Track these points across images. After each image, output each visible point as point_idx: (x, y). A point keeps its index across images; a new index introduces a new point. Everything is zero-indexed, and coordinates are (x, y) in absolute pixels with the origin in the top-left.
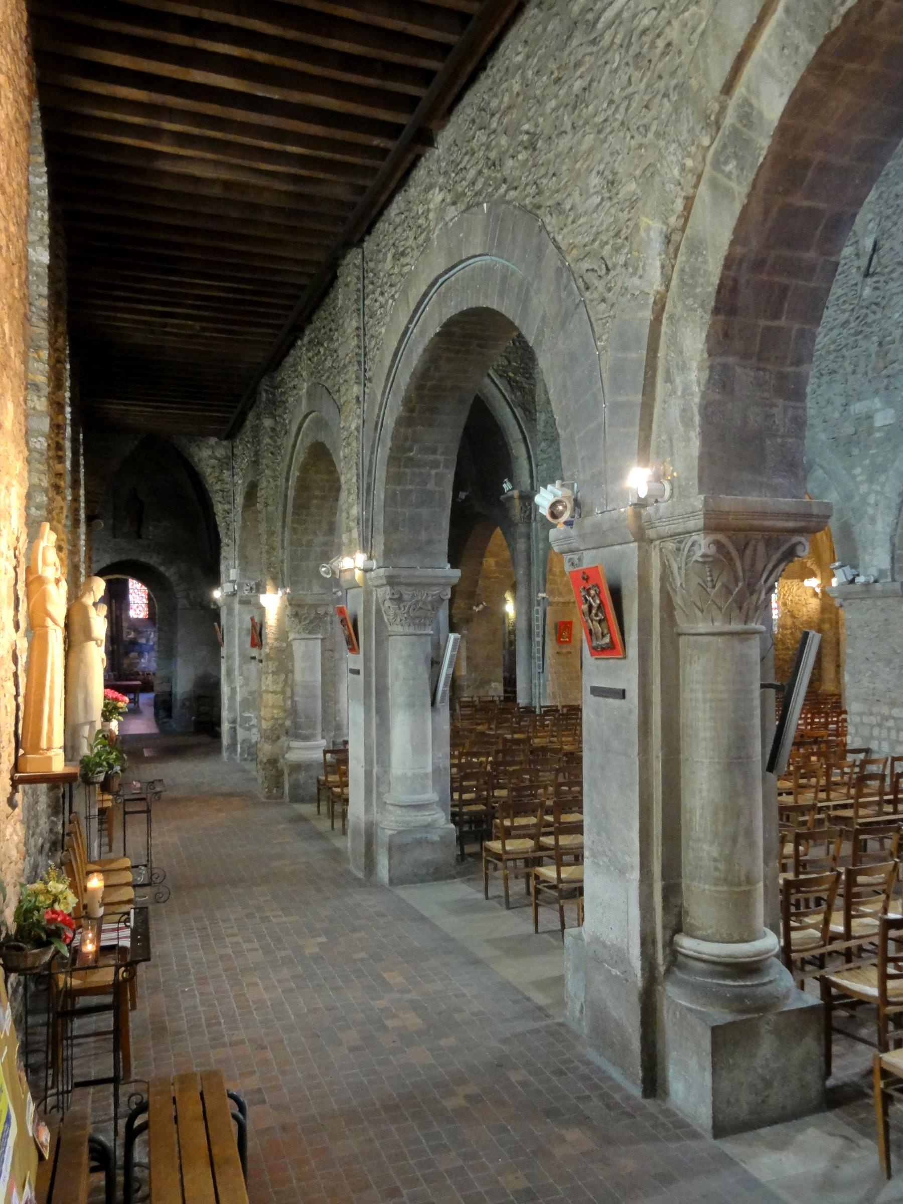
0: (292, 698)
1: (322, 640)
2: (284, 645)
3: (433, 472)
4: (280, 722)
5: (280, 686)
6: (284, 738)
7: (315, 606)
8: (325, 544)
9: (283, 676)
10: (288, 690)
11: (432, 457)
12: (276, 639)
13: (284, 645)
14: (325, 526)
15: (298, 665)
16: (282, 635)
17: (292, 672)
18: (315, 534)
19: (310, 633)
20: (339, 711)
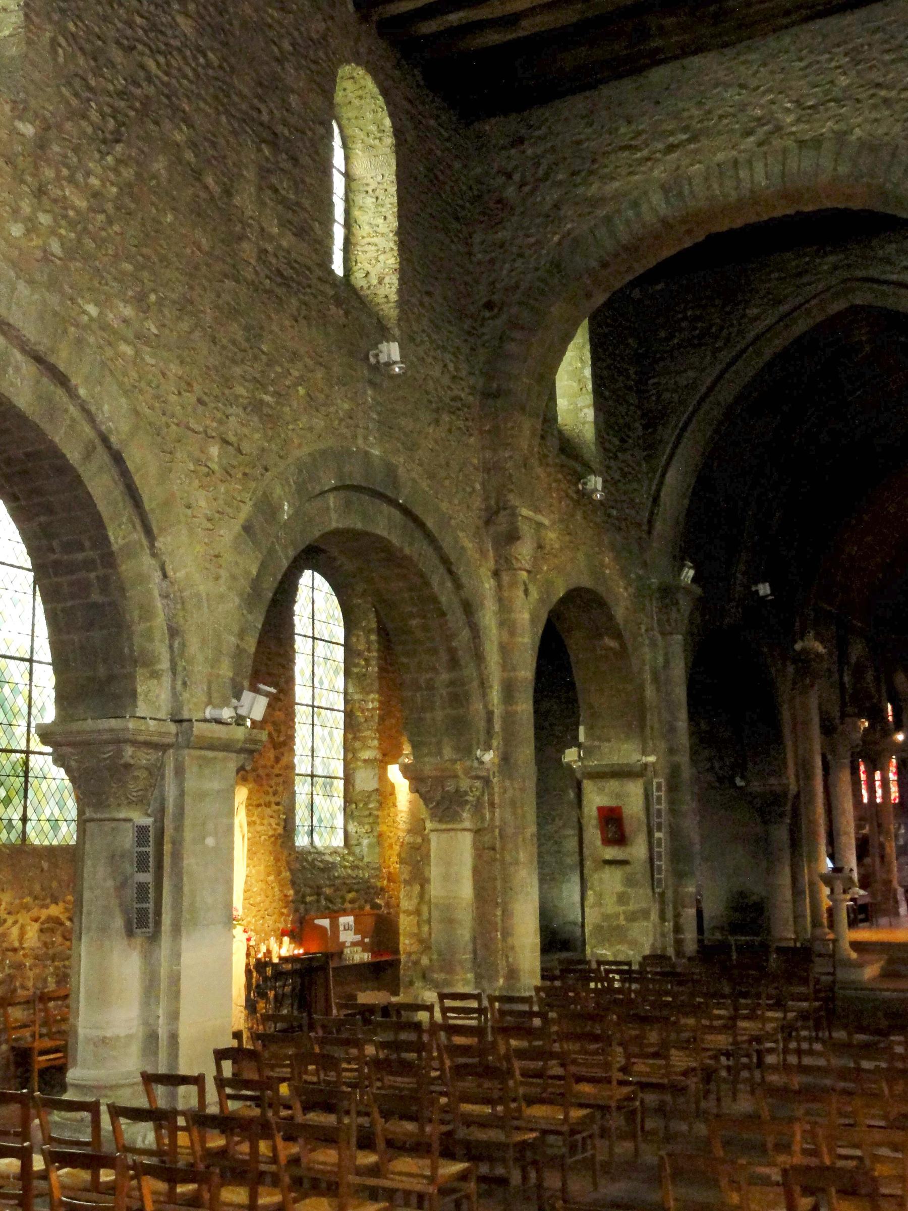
0: (429, 922)
1: (477, 832)
2: (419, 840)
3: (92, 575)
4: (413, 957)
5: (415, 901)
6: (418, 984)
7: (440, 781)
8: (452, 683)
9: (417, 888)
10: (425, 909)
11: (80, 556)
12: (409, 831)
13: (419, 840)
14: (444, 657)
15: (435, 872)
16: (417, 827)
17: (428, 881)
18: (434, 669)
19: (440, 821)
20: (513, 948)
